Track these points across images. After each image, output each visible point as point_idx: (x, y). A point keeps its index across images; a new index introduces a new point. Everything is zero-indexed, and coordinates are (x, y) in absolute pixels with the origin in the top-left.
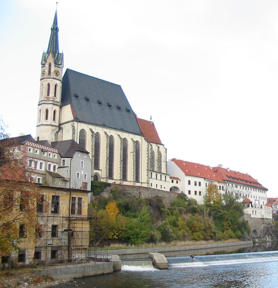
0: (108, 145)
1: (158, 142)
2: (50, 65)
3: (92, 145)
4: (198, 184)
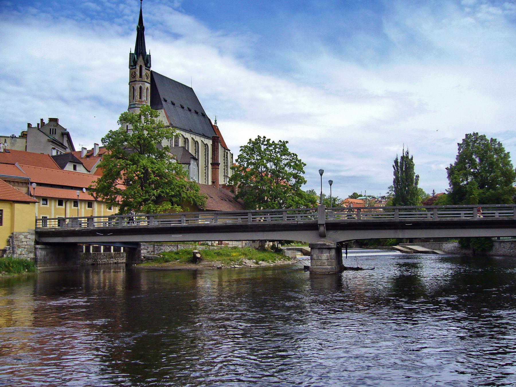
2: (141, 67)
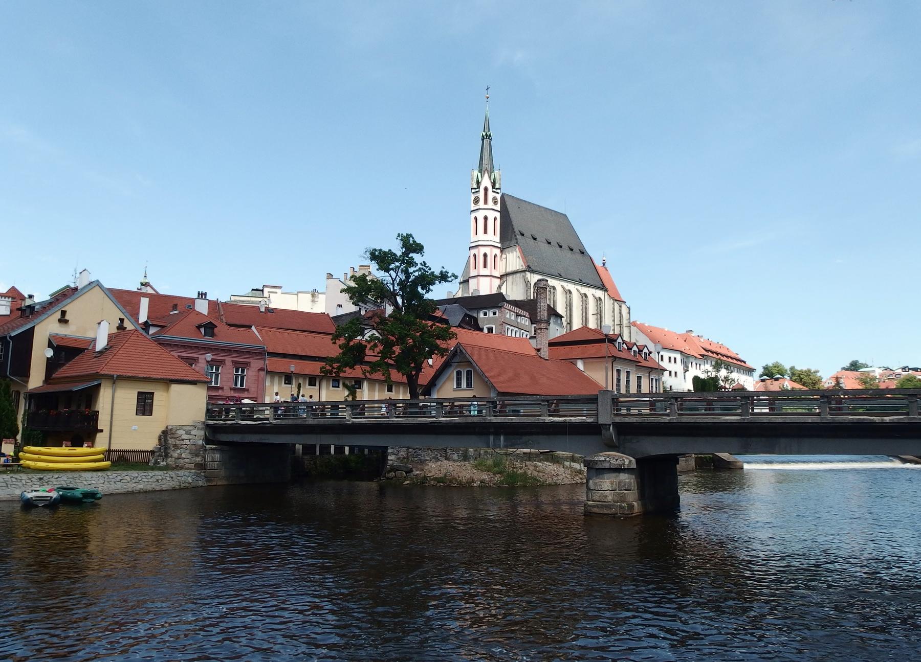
2: (486, 189)
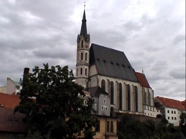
0: (119, 89)
1: (148, 86)
2: (82, 42)
3: (109, 90)
4: (174, 112)
